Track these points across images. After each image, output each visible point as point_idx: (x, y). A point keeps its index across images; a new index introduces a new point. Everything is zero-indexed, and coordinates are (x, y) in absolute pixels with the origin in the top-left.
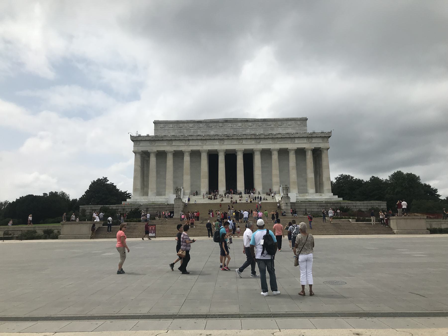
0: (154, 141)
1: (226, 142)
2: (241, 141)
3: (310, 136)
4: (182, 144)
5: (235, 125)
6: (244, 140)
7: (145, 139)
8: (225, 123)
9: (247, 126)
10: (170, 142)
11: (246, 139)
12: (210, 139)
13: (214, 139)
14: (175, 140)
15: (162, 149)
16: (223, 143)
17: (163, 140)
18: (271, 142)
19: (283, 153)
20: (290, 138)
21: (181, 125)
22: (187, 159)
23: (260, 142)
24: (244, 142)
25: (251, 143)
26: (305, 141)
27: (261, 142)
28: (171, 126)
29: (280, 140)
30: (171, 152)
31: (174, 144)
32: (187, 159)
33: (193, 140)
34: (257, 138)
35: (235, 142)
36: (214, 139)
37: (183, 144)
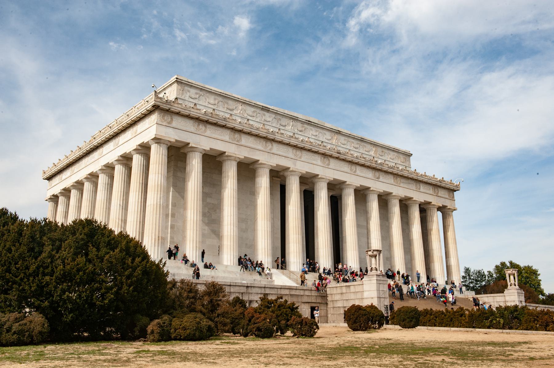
0: (207, 122)
1: (333, 163)
2: (353, 167)
3: (439, 184)
4: (259, 145)
6: (359, 168)
7: (186, 112)
8: (306, 126)
10: (237, 135)
11: (363, 165)
15: (220, 146)
16: (329, 165)
23: (378, 178)
24: (359, 170)
25: (367, 176)
26: (430, 190)
27: (381, 179)
29: (403, 180)
30: (235, 159)
33: (281, 142)
37: (260, 147)
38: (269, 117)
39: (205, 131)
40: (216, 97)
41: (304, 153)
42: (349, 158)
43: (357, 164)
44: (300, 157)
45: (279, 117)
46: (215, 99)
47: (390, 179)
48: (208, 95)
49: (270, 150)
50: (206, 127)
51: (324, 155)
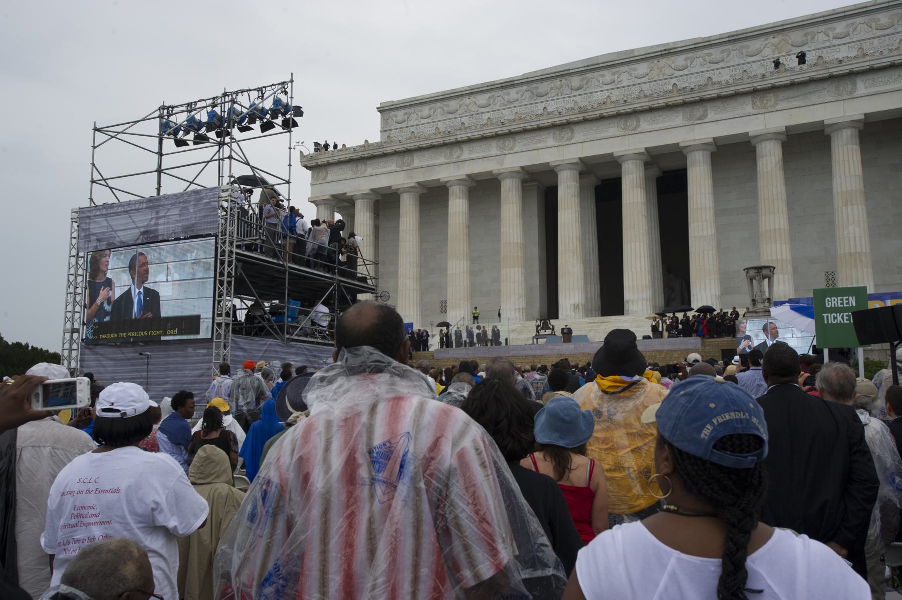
0: (362, 160)
1: (580, 134)
2: (632, 122)
4: (441, 158)
5: (624, 76)
8: (589, 75)
9: (669, 71)
10: (407, 158)
11: (651, 110)
12: (525, 131)
13: (539, 129)
14: (420, 149)
16: (572, 138)
17: (385, 155)
18: (749, 109)
19: (806, 146)
20: (831, 78)
21: (453, 104)
22: (458, 205)
23: (705, 116)
24: (645, 123)
25: (669, 124)
27: (711, 115)
28: (426, 110)
29: (782, 95)
30: (409, 190)
31: (417, 163)
32: (458, 205)
33: (470, 141)
34: (694, 103)
35: (613, 129)
36: (539, 129)
37: (442, 160)
38: (517, 93)
39: (365, 171)
40: (432, 105)
41: (518, 138)
42: (611, 111)
43: (635, 113)
44: (512, 148)
45: (535, 85)
46: (430, 109)
47: (747, 106)
48: (420, 108)
49: (458, 157)
50: (365, 165)
51: (554, 126)
